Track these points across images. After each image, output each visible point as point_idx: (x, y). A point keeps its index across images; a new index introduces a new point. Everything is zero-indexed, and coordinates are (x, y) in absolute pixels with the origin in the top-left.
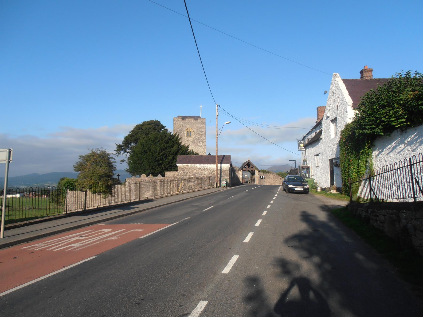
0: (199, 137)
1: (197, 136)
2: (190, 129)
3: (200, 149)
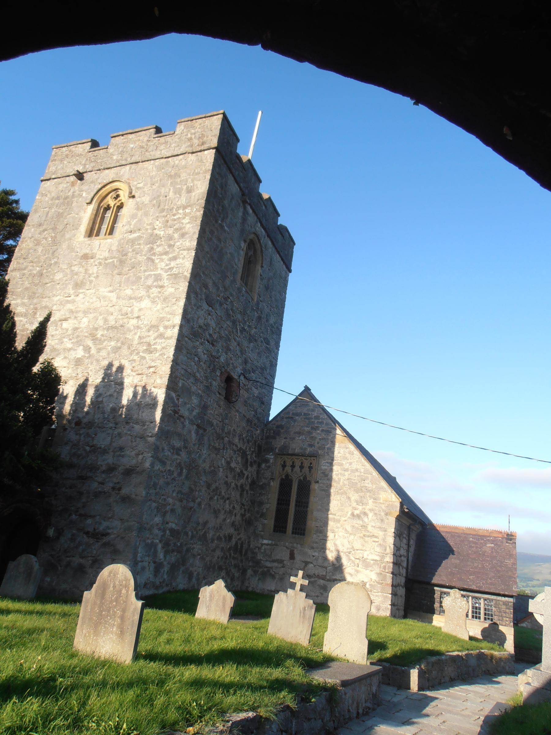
0: (158, 224)
2: (120, 192)
3: (146, 303)
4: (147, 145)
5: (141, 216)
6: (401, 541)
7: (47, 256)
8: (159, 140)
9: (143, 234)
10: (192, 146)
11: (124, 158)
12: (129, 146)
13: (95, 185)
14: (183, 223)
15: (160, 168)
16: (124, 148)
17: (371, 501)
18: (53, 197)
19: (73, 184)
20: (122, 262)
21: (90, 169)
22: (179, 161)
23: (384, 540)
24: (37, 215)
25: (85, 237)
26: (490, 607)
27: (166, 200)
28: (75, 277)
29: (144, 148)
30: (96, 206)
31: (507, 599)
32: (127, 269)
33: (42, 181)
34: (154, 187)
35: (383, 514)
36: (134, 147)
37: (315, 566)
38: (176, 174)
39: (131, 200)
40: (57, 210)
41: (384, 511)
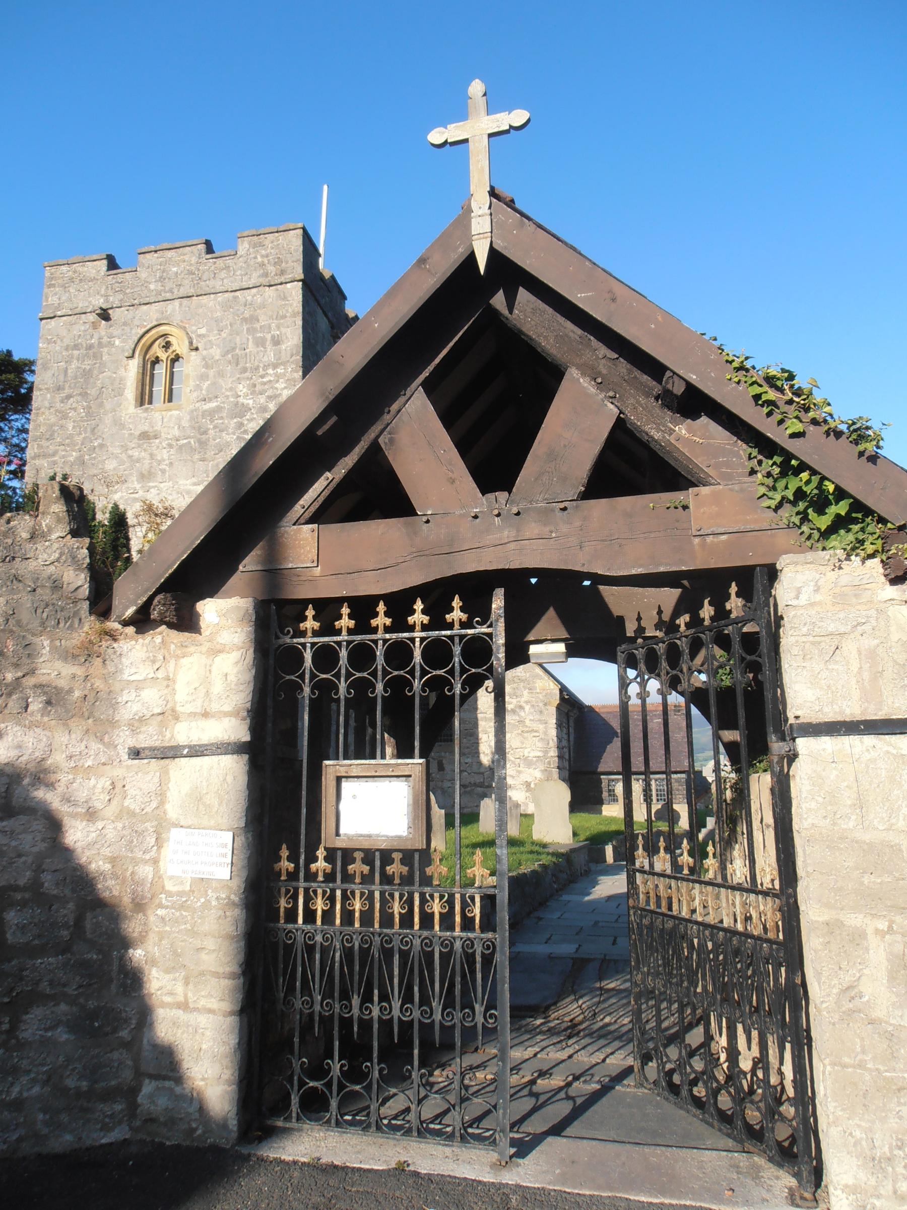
0: (242, 389)
1: (226, 384)
2: (170, 339)
4: (199, 270)
5: (214, 376)
6: (562, 731)
7: (83, 435)
8: (215, 263)
9: (223, 403)
10: (266, 275)
11: (167, 289)
12: (171, 270)
13: (131, 329)
14: (276, 389)
15: (226, 306)
16: (163, 272)
17: (526, 693)
18: (68, 346)
19: (95, 326)
20: (203, 444)
21: (117, 303)
22: (253, 297)
23: (545, 733)
24: (49, 374)
25: (136, 407)
26: (662, 788)
27: (246, 355)
28: (137, 465)
29: (194, 274)
30: (141, 360)
31: (679, 775)
32: (213, 453)
33: (41, 319)
34: (224, 335)
35: (541, 705)
36: (179, 272)
37: (469, 774)
38: (252, 317)
39: (194, 353)
40: (79, 365)
41: (542, 701)
